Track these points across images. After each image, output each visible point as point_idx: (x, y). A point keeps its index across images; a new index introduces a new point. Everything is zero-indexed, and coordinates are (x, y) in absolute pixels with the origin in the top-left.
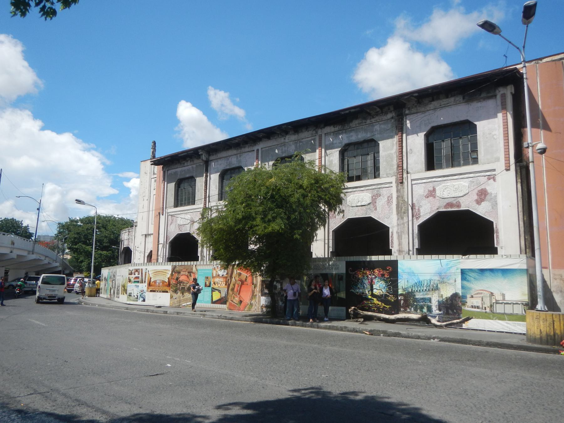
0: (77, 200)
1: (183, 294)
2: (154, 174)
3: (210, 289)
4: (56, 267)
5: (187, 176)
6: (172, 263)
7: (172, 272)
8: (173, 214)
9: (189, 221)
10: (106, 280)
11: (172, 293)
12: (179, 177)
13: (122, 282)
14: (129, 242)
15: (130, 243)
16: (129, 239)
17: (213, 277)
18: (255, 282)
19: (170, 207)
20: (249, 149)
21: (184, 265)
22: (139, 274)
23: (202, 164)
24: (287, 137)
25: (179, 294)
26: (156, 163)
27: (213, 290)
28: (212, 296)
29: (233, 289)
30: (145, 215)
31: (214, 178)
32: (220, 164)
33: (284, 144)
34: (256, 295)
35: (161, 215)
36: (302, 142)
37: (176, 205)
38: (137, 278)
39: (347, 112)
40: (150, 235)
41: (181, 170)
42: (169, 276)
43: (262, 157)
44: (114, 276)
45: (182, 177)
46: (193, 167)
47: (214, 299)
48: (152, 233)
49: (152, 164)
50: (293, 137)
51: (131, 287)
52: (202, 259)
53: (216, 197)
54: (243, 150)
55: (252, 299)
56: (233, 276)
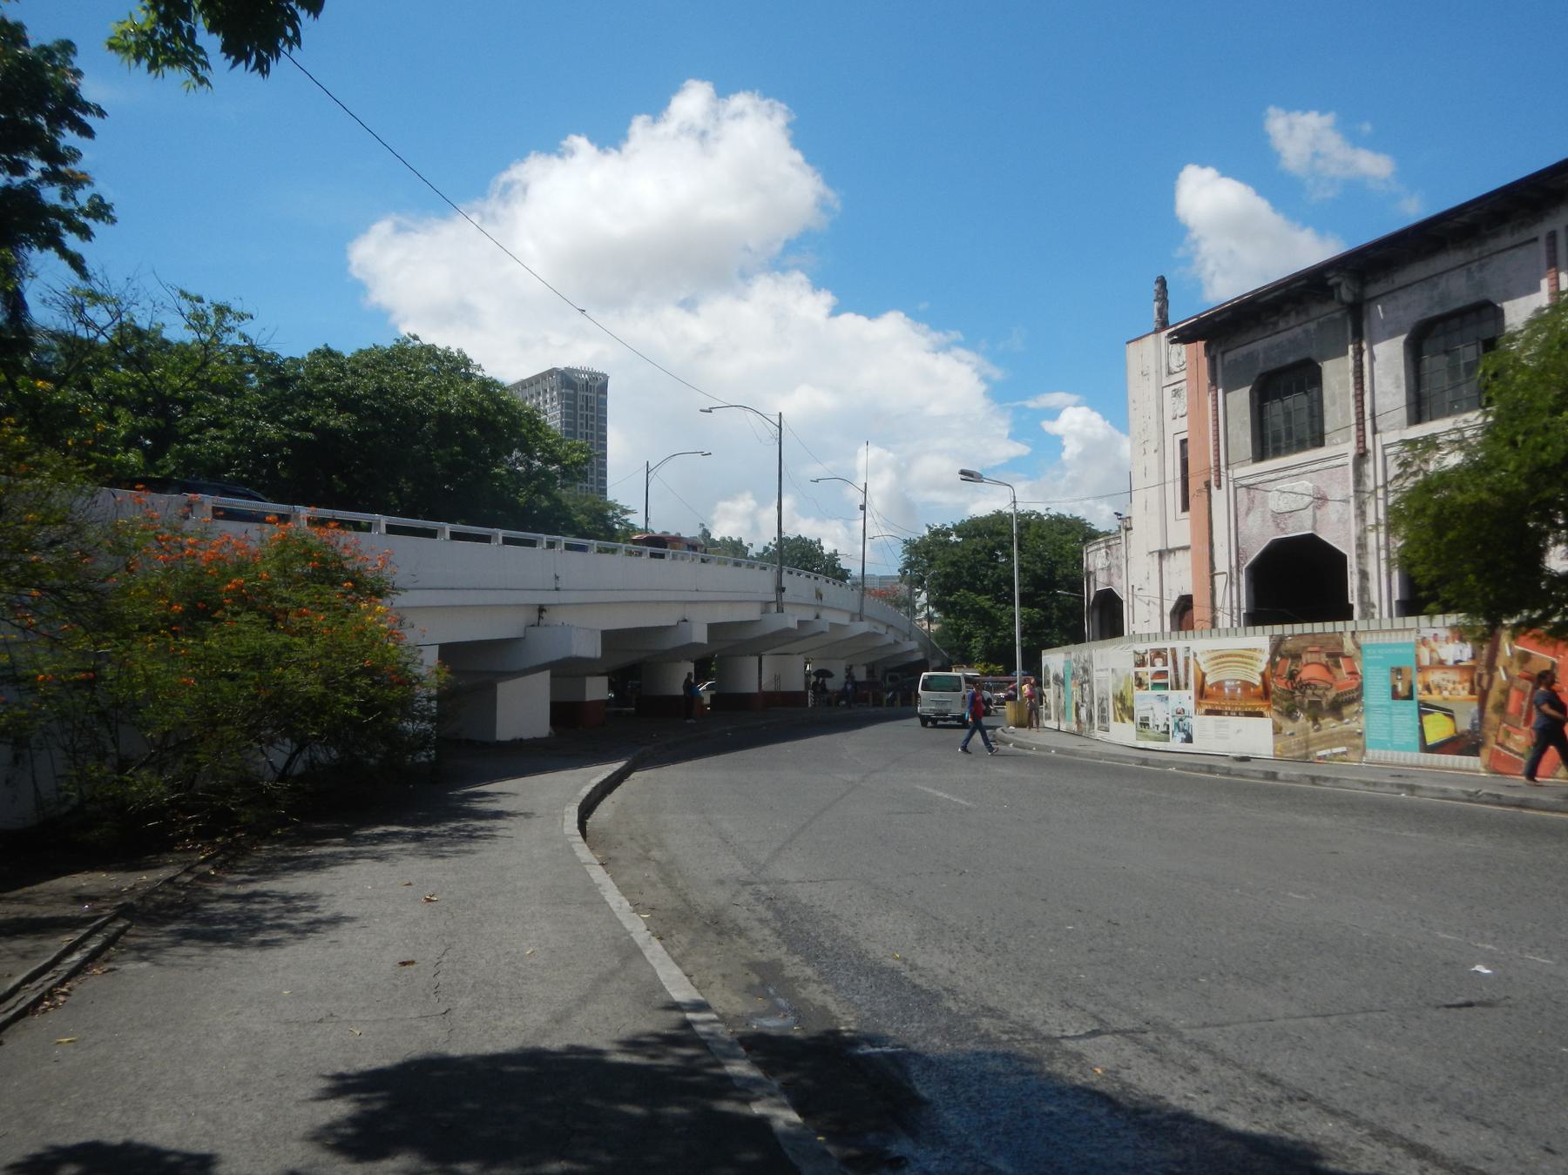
0: (962, 472)
1: (1315, 721)
2: (1170, 373)
3: (1412, 706)
4: (912, 652)
5: (1291, 360)
6: (1268, 628)
8: (1251, 481)
9: (1308, 499)
10: (1059, 681)
11: (1279, 720)
12: (1262, 367)
13: (1116, 686)
14: (1110, 575)
15: (1115, 579)
16: (1109, 568)
17: (1421, 669)
19: (1242, 463)
20: (1518, 238)
21: (1313, 634)
22: (1165, 664)
26: (1185, 336)
27: (1425, 709)
28: (1421, 728)
29: (1501, 708)
30: (1154, 494)
31: (1388, 358)
35: (1214, 489)
37: (1260, 454)
38: (1163, 674)
40: (1172, 551)
41: (1267, 348)
42: (1262, 666)
44: (1086, 671)
45: (1273, 366)
46: (1306, 331)
47: (1432, 739)
48: (1187, 542)
49: (1173, 342)
51: (1144, 702)
52: (1366, 615)
53: (1402, 414)
54: (1492, 245)
56: (1500, 663)
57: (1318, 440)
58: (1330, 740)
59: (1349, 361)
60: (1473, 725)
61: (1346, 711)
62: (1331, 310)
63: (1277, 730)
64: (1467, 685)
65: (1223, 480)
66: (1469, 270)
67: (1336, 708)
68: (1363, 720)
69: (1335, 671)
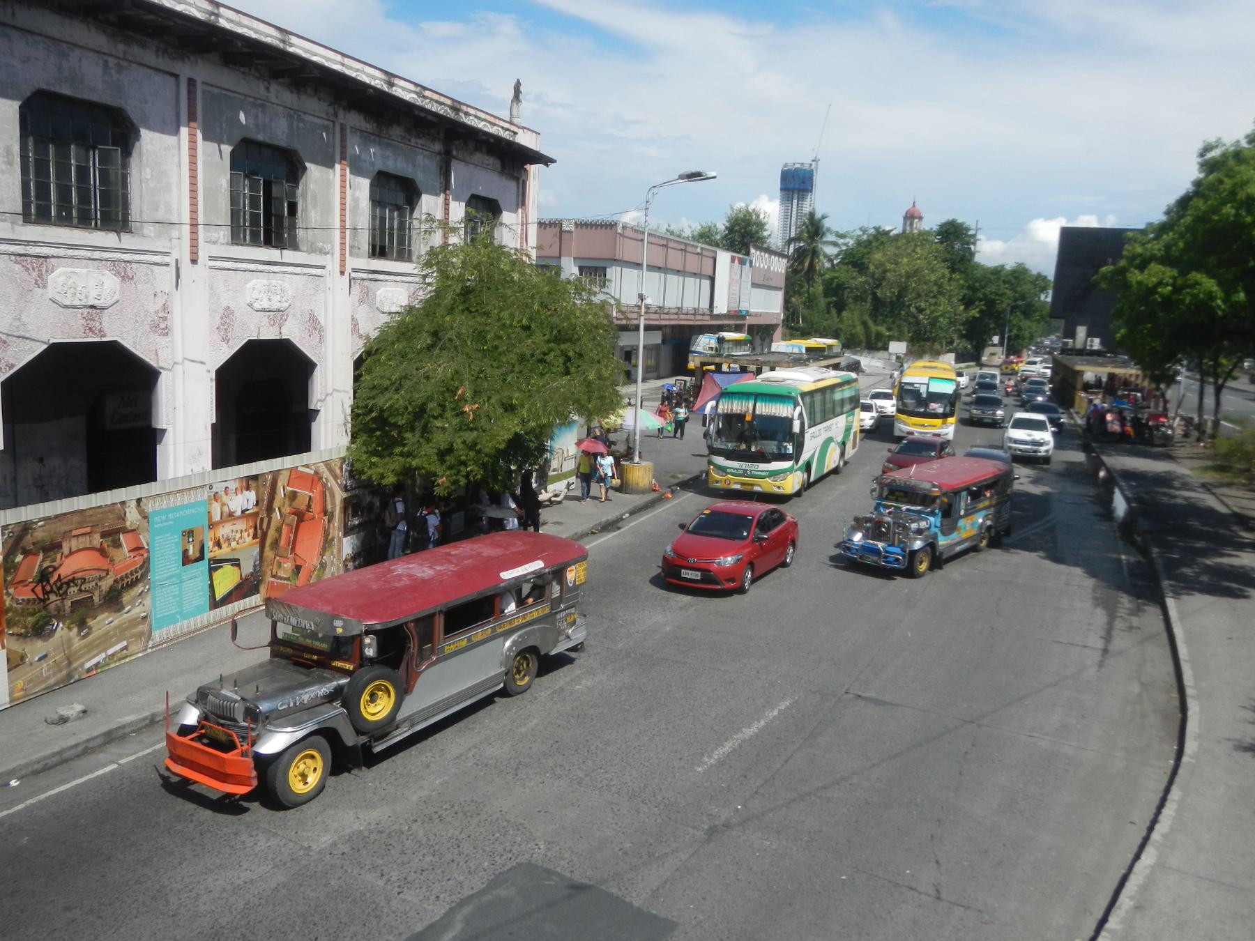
1: (82, 624)
3: (203, 566)
11: (16, 646)
17: (212, 525)
18: (329, 507)
24: (274, 87)
25: (62, 631)
28: (212, 586)
29: (276, 543)
32: (26, 60)
33: (262, 105)
34: (333, 539)
36: (303, 121)
39: (422, 115)
50: (289, 98)
54: (136, 50)
55: (322, 555)
56: (276, 506)
58: (106, 640)
60: (255, 566)
61: (126, 598)
66: (106, 62)
67: (113, 600)
68: (148, 601)
69: (113, 552)
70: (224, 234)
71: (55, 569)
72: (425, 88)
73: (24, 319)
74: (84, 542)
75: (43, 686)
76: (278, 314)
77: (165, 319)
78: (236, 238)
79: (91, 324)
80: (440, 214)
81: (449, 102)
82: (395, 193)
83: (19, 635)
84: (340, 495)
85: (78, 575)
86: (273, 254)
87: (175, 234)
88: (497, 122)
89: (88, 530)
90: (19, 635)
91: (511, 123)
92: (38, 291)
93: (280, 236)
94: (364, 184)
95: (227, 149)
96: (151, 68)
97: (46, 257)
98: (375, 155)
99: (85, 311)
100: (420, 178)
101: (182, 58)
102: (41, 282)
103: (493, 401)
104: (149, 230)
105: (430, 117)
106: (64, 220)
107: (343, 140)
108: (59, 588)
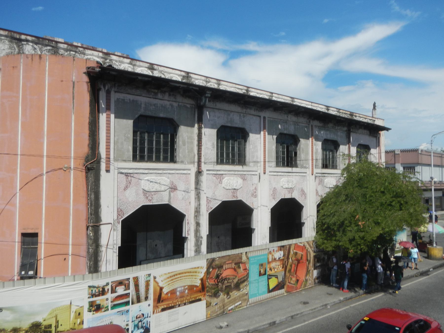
1: (228, 294)
3: (265, 277)
5: (162, 115)
7: (208, 269)
11: (209, 299)
12: (142, 111)
18: (309, 258)
23: (189, 106)
24: (290, 116)
25: (222, 296)
28: (268, 284)
29: (290, 271)
31: (210, 135)
32: (219, 118)
33: (286, 122)
34: (310, 270)
39: (340, 118)
42: (202, 275)
43: (268, 128)
45: (149, 113)
50: (294, 119)
54: (248, 111)
55: (306, 276)
57: (173, 160)
58: (235, 301)
59: (195, 129)
60: (283, 278)
62: (189, 102)
63: (208, 305)
64: (282, 265)
65: (112, 168)
66: (240, 115)
67: (237, 287)
68: (248, 288)
70: (274, 164)
71: (221, 274)
72: (340, 109)
73: (216, 193)
74: (229, 266)
75: (216, 314)
76: (291, 190)
77: (255, 192)
78: (278, 165)
79: (234, 194)
80: (347, 152)
81: (349, 113)
82: (330, 146)
83: (210, 296)
84: (312, 254)
85: (227, 277)
86: (289, 169)
87: (259, 165)
88: (367, 117)
89: (231, 262)
90: (210, 296)
91: (372, 117)
92: (220, 185)
93: (292, 163)
94: (320, 144)
95: (275, 137)
96: (253, 115)
97: (222, 174)
98: (323, 134)
99: (232, 191)
100: (339, 140)
101: (261, 111)
102: (221, 182)
103: (370, 220)
104: (251, 164)
105: (342, 119)
106: (228, 163)
107: (312, 130)
108: (222, 281)
